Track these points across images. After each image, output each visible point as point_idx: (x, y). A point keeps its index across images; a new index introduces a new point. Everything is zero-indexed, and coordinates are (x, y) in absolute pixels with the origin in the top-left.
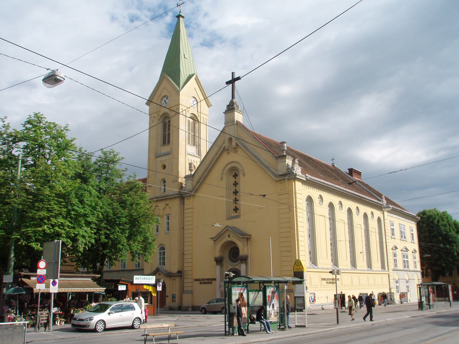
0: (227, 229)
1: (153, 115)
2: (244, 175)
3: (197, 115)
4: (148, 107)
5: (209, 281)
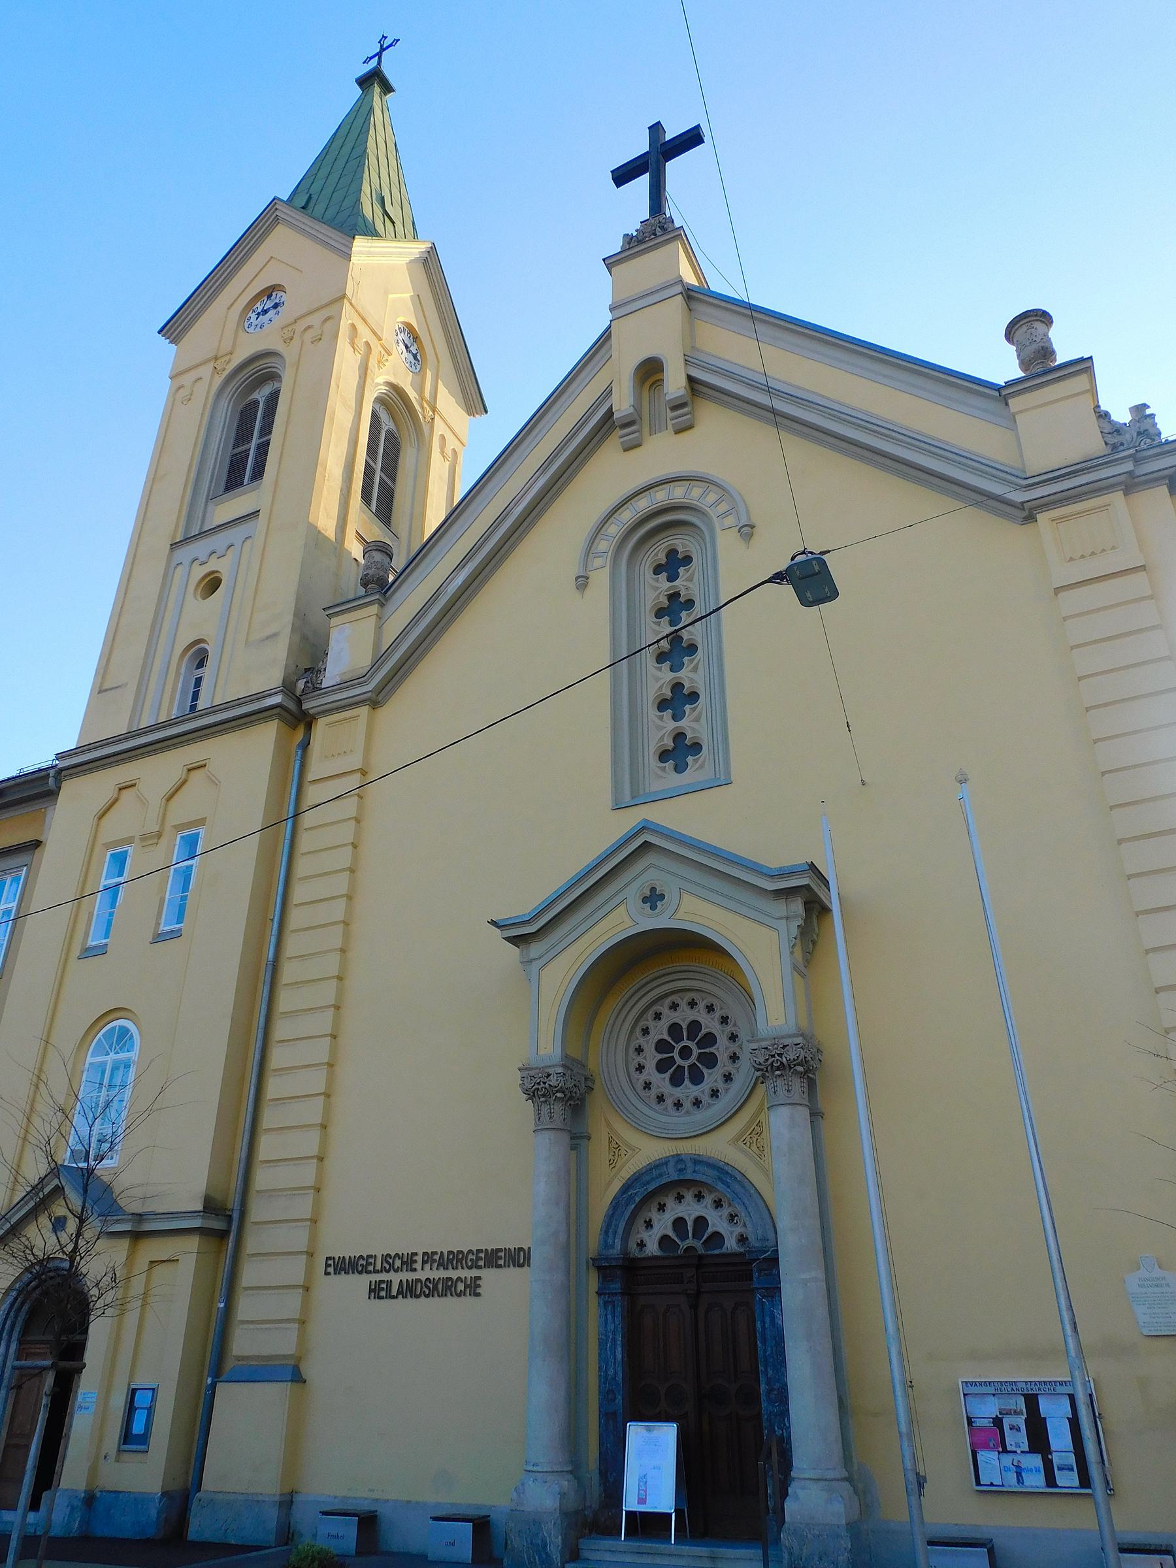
0: (640, 847)
5: (453, 1274)
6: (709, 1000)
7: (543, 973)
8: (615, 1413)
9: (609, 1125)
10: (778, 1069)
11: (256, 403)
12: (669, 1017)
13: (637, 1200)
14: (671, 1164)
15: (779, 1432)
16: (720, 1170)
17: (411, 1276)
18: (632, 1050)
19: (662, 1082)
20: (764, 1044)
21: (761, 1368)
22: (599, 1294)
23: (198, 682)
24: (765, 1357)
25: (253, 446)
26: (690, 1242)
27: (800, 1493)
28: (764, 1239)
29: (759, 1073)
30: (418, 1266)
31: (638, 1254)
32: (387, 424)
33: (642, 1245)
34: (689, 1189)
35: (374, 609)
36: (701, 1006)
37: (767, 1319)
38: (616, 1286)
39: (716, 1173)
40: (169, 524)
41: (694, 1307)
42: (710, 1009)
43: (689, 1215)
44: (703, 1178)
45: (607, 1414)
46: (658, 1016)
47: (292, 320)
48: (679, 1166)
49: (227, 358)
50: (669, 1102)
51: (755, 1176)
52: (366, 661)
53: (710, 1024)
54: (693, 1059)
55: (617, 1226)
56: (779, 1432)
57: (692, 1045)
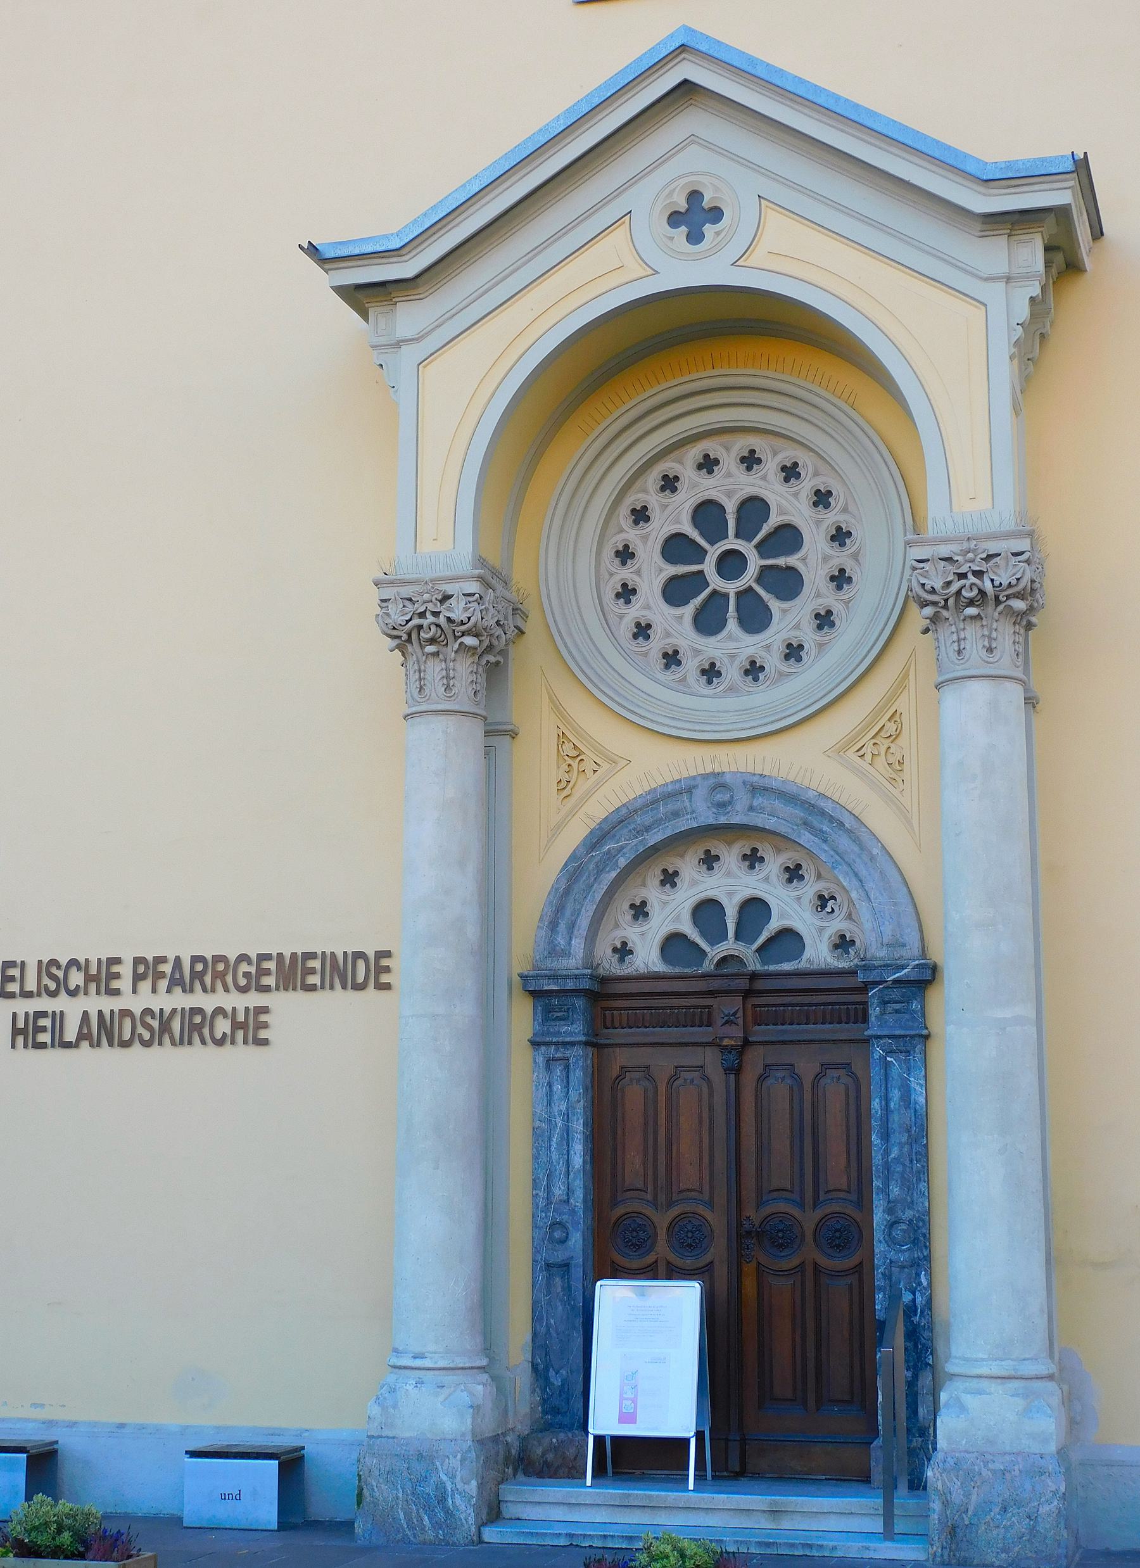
5: (199, 1000)
6: (789, 454)
7: (431, 372)
8: (565, 1266)
9: (557, 708)
10: (971, 603)
12: (696, 487)
13: (622, 862)
14: (700, 794)
15: (907, 1297)
16: (810, 807)
17: (108, 1005)
18: (608, 553)
19: (675, 625)
20: (944, 550)
21: (877, 1183)
22: (535, 1044)
24: (887, 1166)
26: (730, 946)
27: (969, 1400)
28: (896, 944)
29: (929, 611)
30: (124, 984)
31: (618, 970)
33: (623, 951)
34: (730, 844)
36: (771, 466)
37: (895, 1094)
38: (575, 1030)
39: (799, 813)
41: (735, 1071)
42: (790, 472)
43: (730, 895)
44: (770, 823)
45: (549, 1266)
46: (669, 484)
48: (720, 797)
50: (691, 666)
51: (881, 821)
53: (788, 505)
54: (748, 578)
55: (577, 913)
56: (907, 1297)
57: (747, 548)
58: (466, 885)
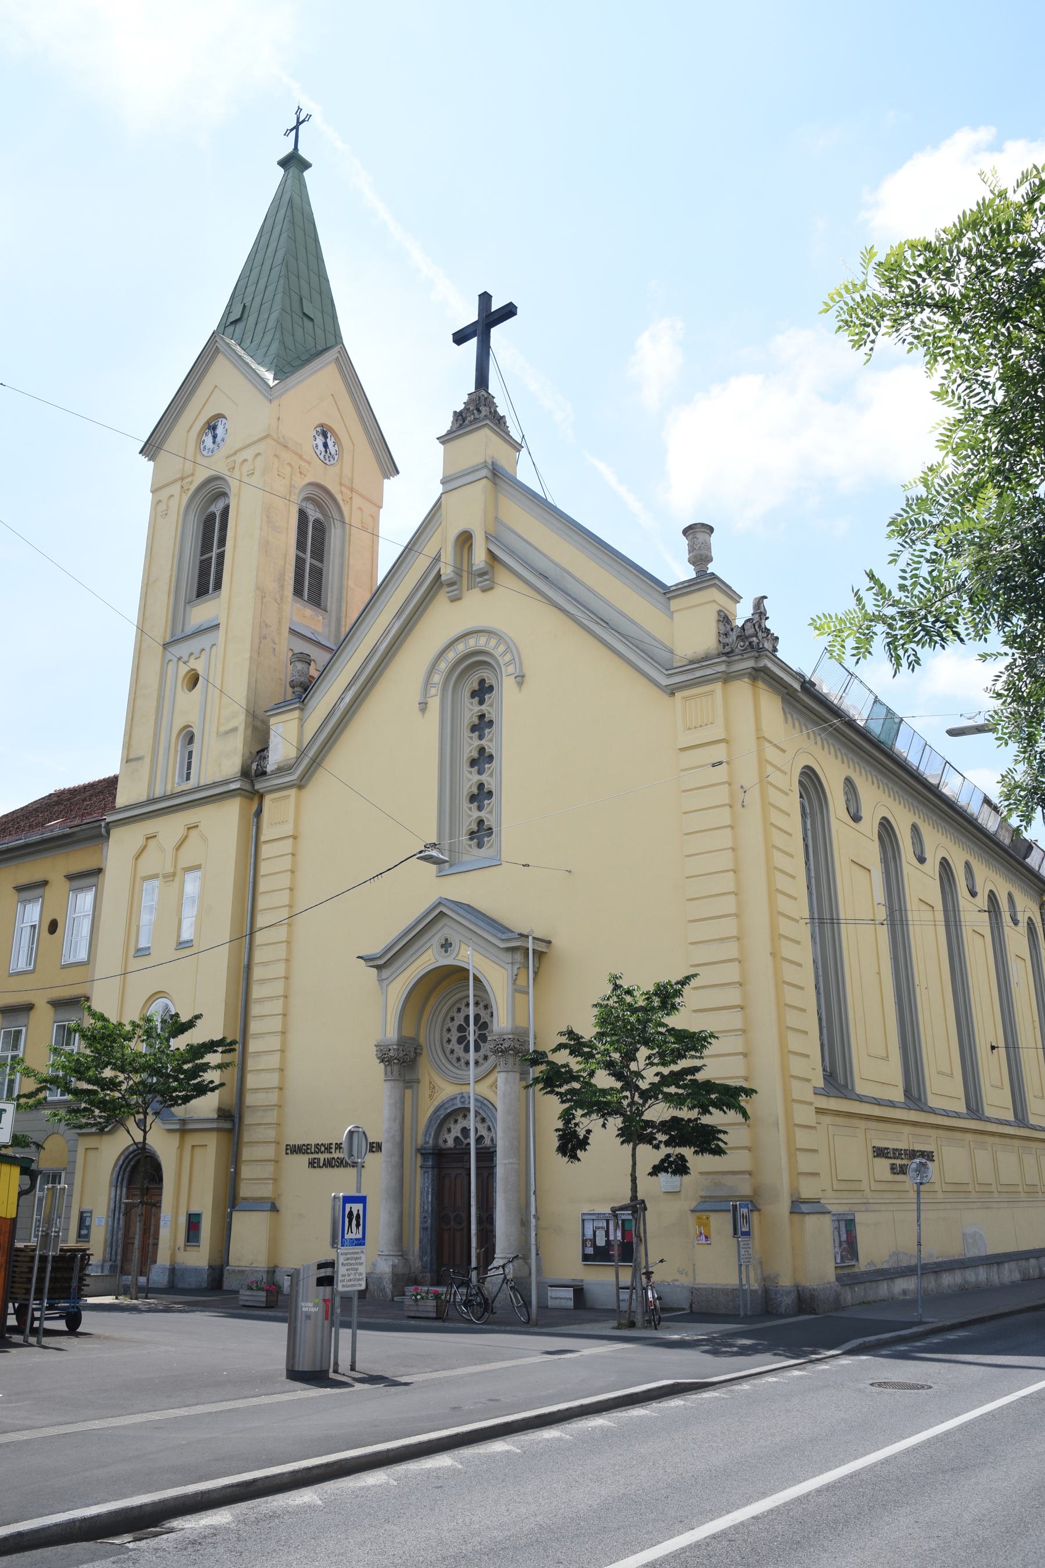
0: (437, 916)
1: (164, 494)
2: (520, 679)
3: (339, 498)
4: (152, 463)
11: (213, 515)
17: (329, 1156)
18: (445, 1030)
22: (421, 1167)
23: (190, 753)
25: (214, 554)
30: (333, 1150)
31: (443, 1146)
32: (313, 514)
33: (445, 1141)
35: (296, 714)
40: (160, 631)
47: (232, 452)
49: (190, 479)
52: (293, 753)
58: (396, 1126)
